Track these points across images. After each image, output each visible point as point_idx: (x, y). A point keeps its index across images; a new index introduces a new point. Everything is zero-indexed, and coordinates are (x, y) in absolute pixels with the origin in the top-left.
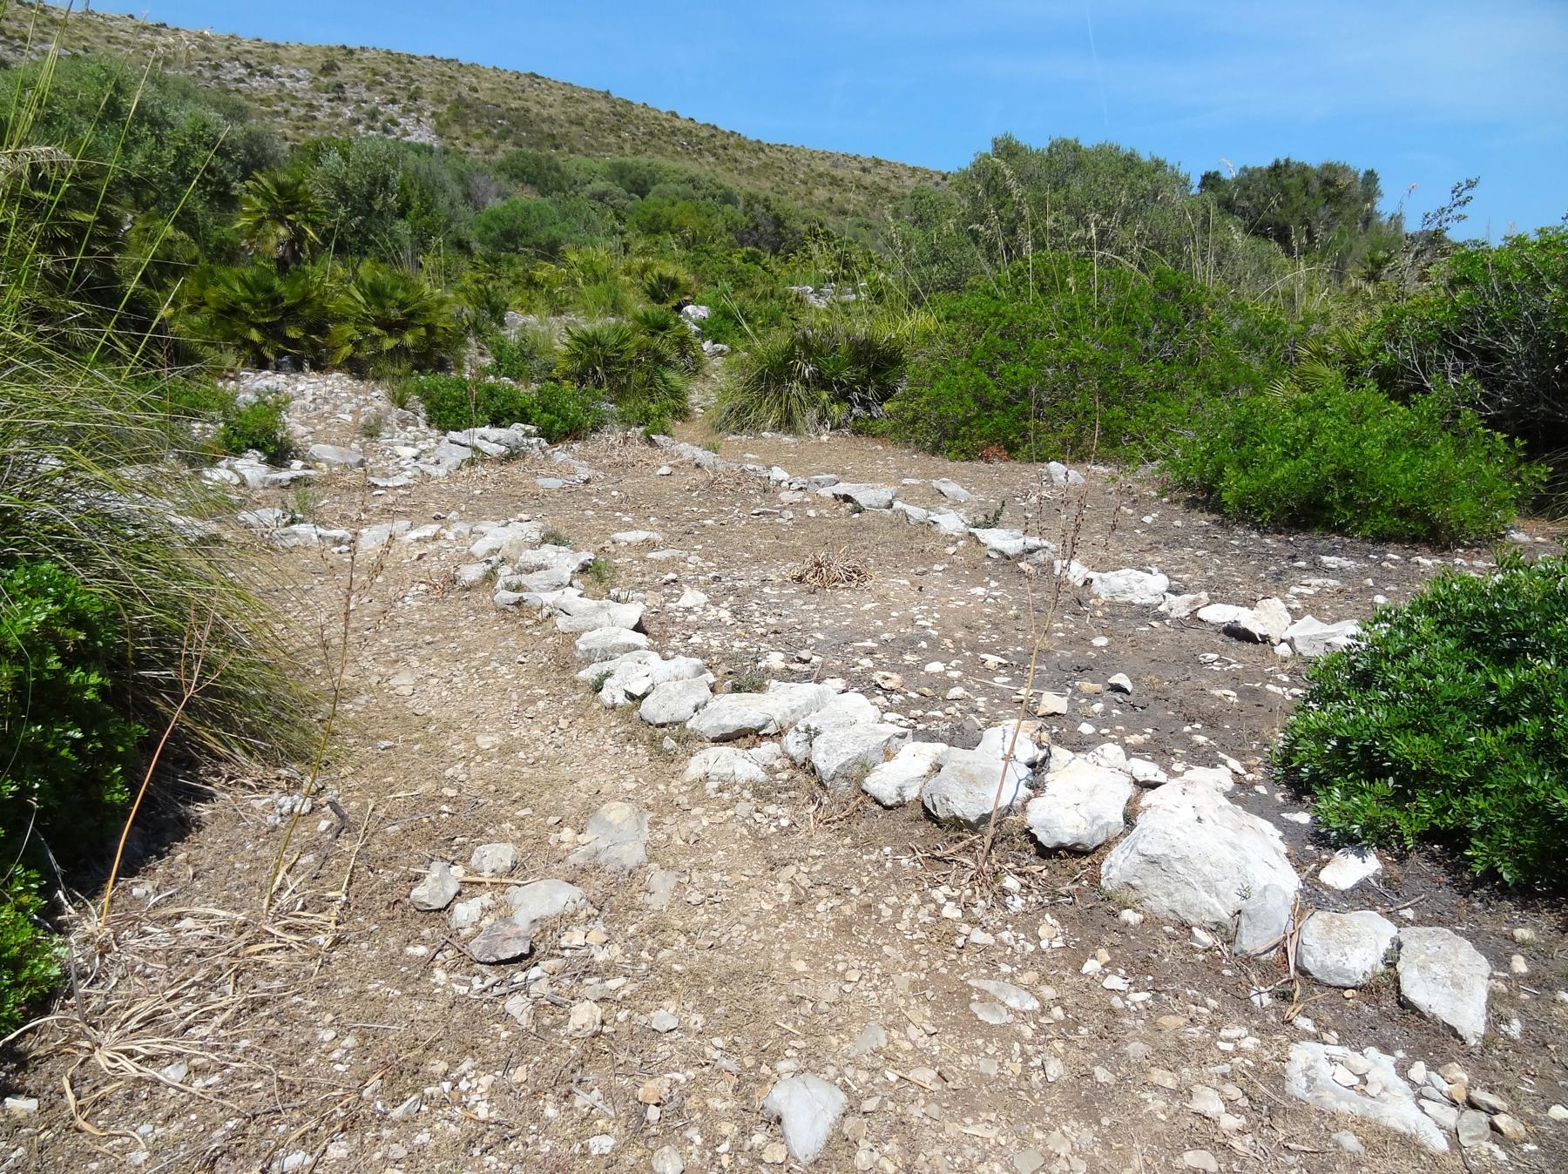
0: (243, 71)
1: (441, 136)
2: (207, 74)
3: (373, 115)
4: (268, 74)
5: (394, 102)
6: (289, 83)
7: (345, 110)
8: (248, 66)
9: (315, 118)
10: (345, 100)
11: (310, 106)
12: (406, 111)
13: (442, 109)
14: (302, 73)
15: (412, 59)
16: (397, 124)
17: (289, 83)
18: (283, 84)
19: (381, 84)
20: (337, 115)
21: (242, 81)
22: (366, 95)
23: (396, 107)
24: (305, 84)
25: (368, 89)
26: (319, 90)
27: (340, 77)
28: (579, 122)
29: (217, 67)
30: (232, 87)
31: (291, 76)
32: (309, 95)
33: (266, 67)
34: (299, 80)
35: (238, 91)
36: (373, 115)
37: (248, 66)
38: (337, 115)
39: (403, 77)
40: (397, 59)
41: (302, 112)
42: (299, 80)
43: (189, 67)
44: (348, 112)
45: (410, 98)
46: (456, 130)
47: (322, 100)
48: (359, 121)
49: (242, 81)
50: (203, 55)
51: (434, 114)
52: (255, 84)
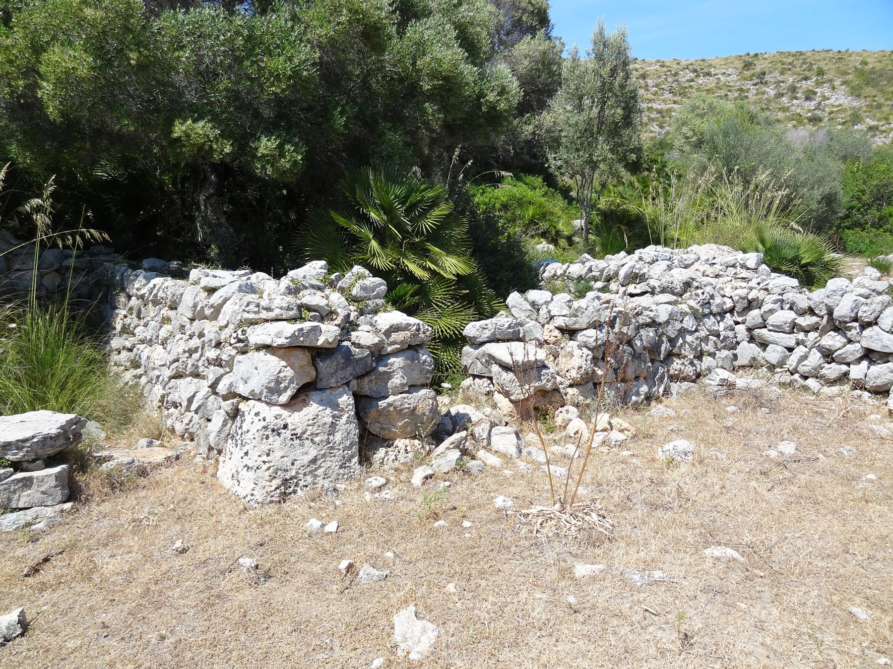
0: (692, 75)
1: (858, 96)
2: (670, 80)
3: (793, 89)
4: (709, 74)
5: (806, 79)
6: (722, 78)
8: (695, 71)
9: (747, 97)
10: (766, 83)
11: (741, 90)
12: (818, 84)
13: (850, 77)
14: (730, 71)
15: (801, 54)
16: (815, 93)
17: (722, 78)
18: (719, 79)
20: (763, 93)
21: (692, 80)
22: (781, 78)
23: (809, 82)
24: (734, 77)
25: (782, 73)
26: (745, 79)
27: (758, 69)
29: (676, 74)
30: (686, 85)
31: (724, 73)
32: (738, 84)
33: (706, 70)
34: (730, 75)
35: (691, 87)
36: (793, 89)
37: (695, 71)
38: (763, 93)
39: (804, 63)
40: (789, 54)
41: (736, 94)
42: (730, 75)
43: (659, 77)
44: (771, 92)
46: (869, 90)
47: (748, 85)
48: (783, 95)
49: (692, 80)
50: (665, 69)
51: (843, 83)
52: (700, 82)
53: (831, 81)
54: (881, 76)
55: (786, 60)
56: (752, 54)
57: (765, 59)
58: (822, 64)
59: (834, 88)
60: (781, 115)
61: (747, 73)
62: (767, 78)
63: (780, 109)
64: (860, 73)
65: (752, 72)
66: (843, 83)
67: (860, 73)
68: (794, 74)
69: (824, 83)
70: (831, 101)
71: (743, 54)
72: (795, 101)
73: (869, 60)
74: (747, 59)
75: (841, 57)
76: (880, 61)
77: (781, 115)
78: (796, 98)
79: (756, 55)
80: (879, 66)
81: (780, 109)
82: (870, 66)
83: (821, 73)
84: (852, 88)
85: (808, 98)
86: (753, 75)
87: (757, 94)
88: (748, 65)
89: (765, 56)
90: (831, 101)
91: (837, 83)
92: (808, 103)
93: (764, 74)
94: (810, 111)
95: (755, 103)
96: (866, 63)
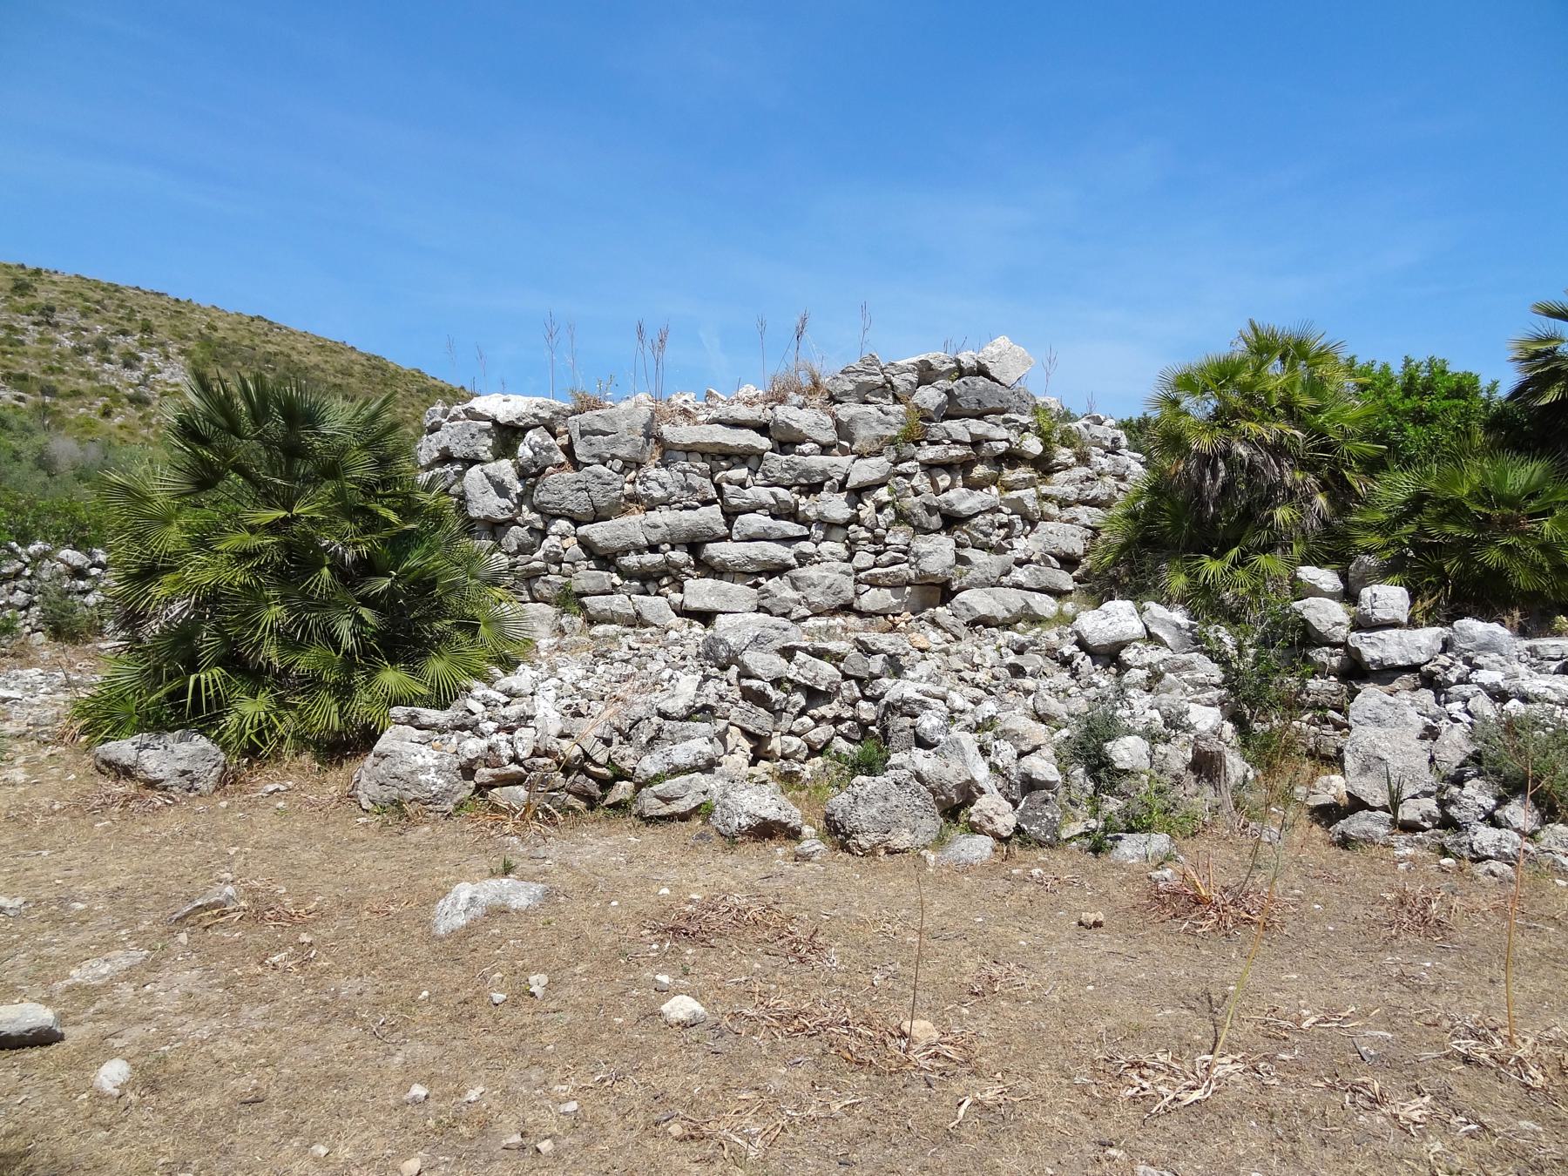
3: (103, 346)
5: (125, 333)
7: (58, 336)
9: (22, 343)
10: (56, 326)
11: (11, 328)
12: (144, 345)
15: (117, 289)
16: (140, 359)
19: (97, 311)
20: (52, 341)
22: (83, 323)
23: (129, 339)
25: (84, 315)
26: (18, 311)
27: (42, 297)
28: (346, 372)
36: (103, 346)
40: (97, 285)
45: (143, 331)
47: (23, 322)
48: (86, 352)
53: (162, 344)
54: (233, 352)
55: (90, 294)
56: (31, 266)
57: (54, 283)
58: (150, 315)
59: (167, 358)
60: (83, 384)
61: (22, 302)
62: (58, 317)
63: (82, 374)
64: (206, 341)
65: (32, 301)
66: (182, 352)
67: (206, 341)
68: (105, 320)
69: (152, 345)
70: (165, 376)
71: (13, 262)
72: (107, 366)
73: (219, 324)
74: (21, 274)
75: (179, 310)
76: (234, 330)
77: (83, 384)
78: (109, 361)
79: (38, 272)
80: (232, 337)
81: (82, 374)
82: (220, 334)
83: (147, 328)
84: (194, 362)
85: (127, 365)
86: (33, 307)
87: (41, 341)
88: (21, 288)
89: (55, 278)
90: (165, 376)
91: (172, 350)
92: (127, 373)
93: (52, 310)
94: (131, 385)
95: (37, 356)
96: (216, 330)
